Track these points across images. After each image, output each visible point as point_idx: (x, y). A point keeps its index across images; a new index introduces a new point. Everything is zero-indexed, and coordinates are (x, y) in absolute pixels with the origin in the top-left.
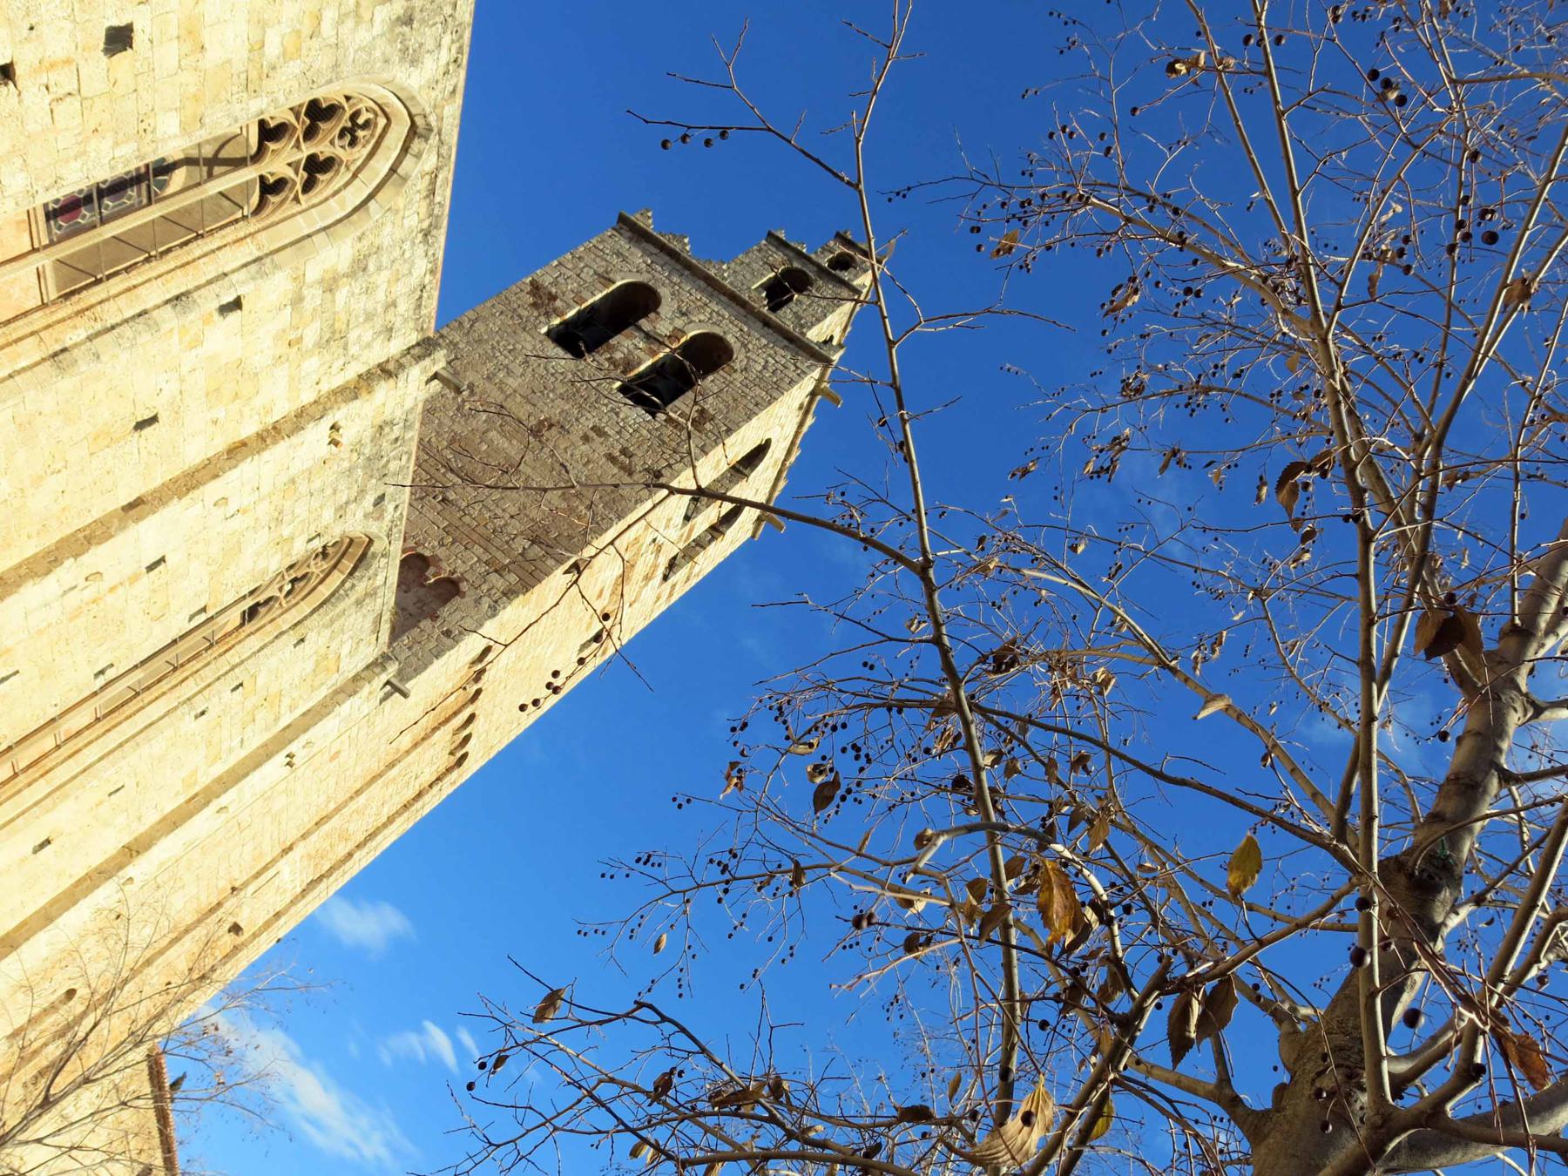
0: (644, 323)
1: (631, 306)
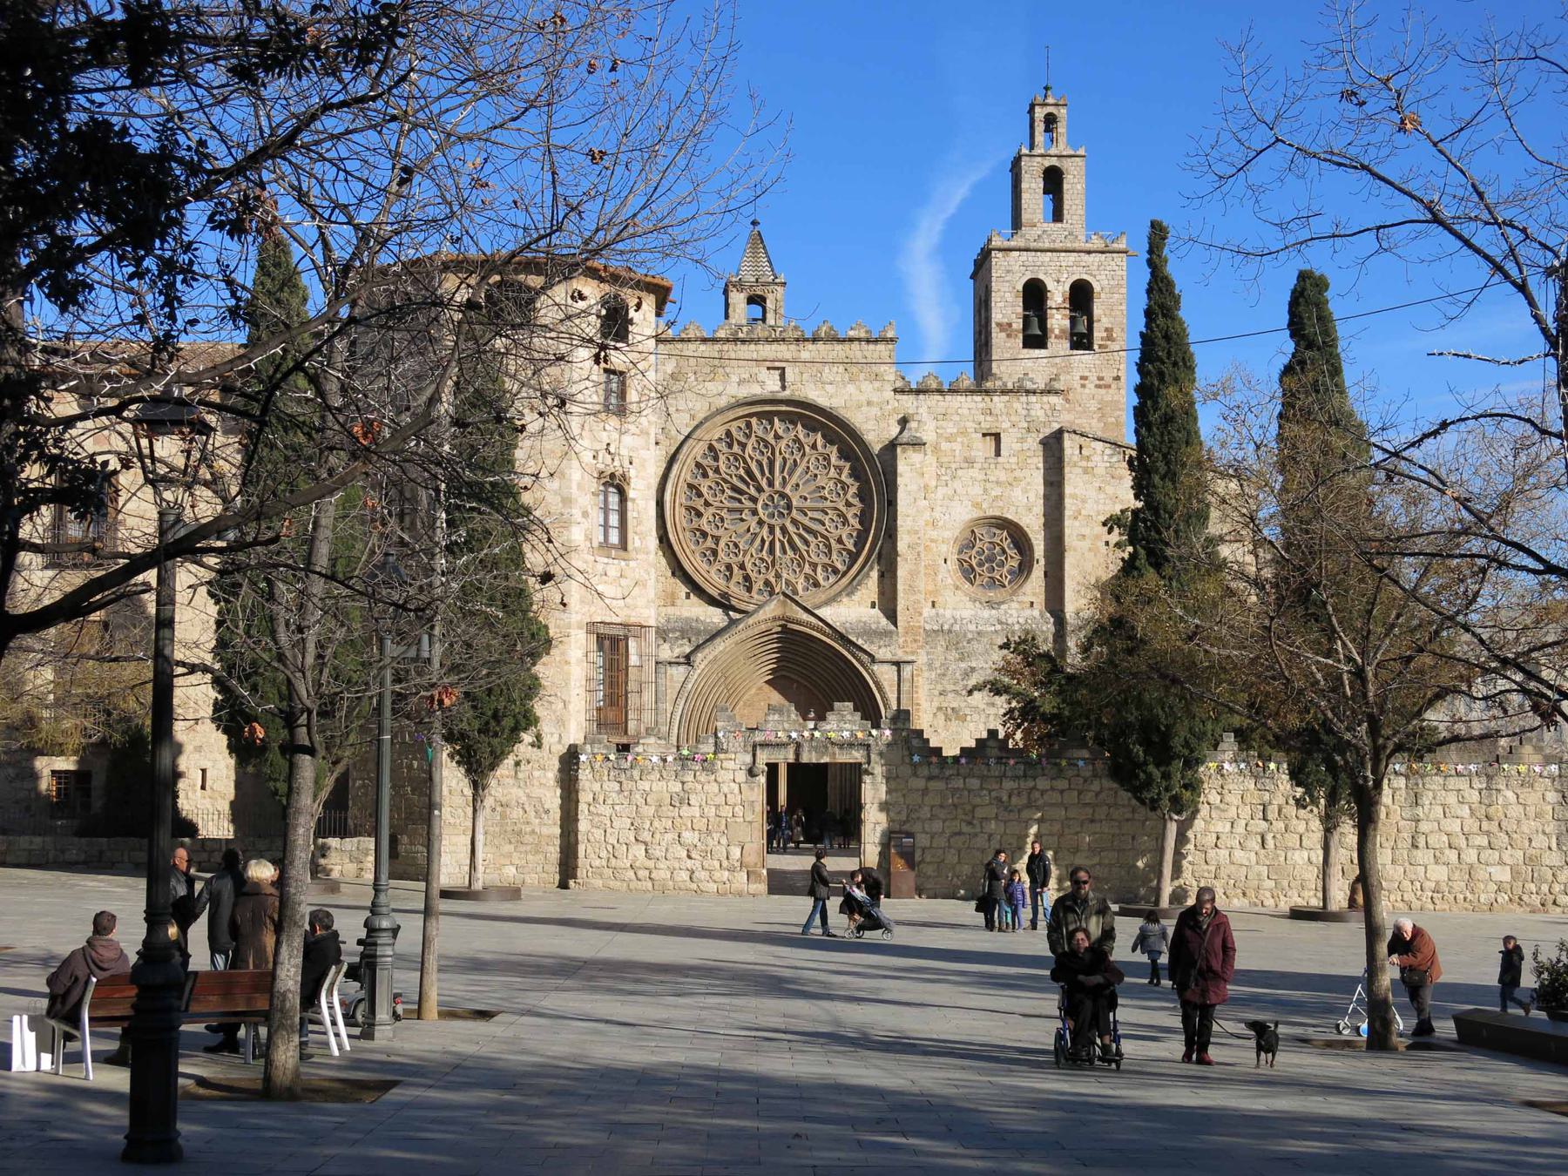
0: (1050, 303)
1: (1034, 294)
